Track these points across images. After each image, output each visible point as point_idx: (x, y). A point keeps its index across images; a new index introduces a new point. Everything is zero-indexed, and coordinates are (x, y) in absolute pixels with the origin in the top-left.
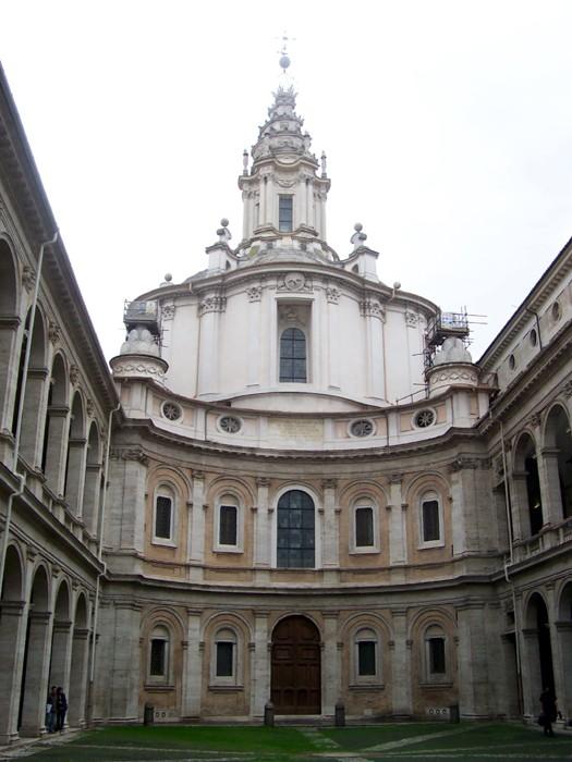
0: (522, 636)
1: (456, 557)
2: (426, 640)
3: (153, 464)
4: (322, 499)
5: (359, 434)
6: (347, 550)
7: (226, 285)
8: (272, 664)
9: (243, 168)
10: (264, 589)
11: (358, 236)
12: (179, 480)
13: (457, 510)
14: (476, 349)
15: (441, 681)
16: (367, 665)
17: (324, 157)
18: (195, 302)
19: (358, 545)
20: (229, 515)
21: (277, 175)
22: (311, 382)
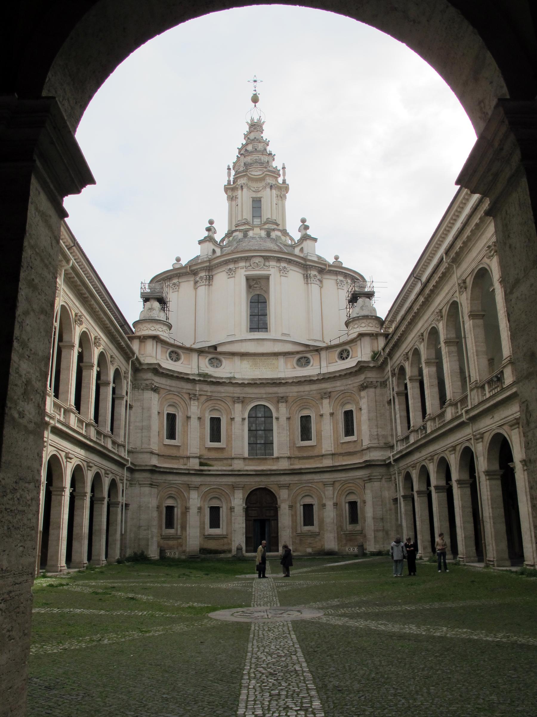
0: (402, 500)
1: (364, 447)
3: (162, 392)
4: (278, 409)
5: (301, 366)
6: (294, 444)
8: (246, 520)
10: (239, 471)
11: (303, 226)
12: (182, 403)
14: (382, 306)
15: (356, 529)
16: (308, 519)
17: (284, 168)
18: (192, 279)
19: (302, 440)
20: (216, 423)
21: (250, 184)
22: (270, 331)
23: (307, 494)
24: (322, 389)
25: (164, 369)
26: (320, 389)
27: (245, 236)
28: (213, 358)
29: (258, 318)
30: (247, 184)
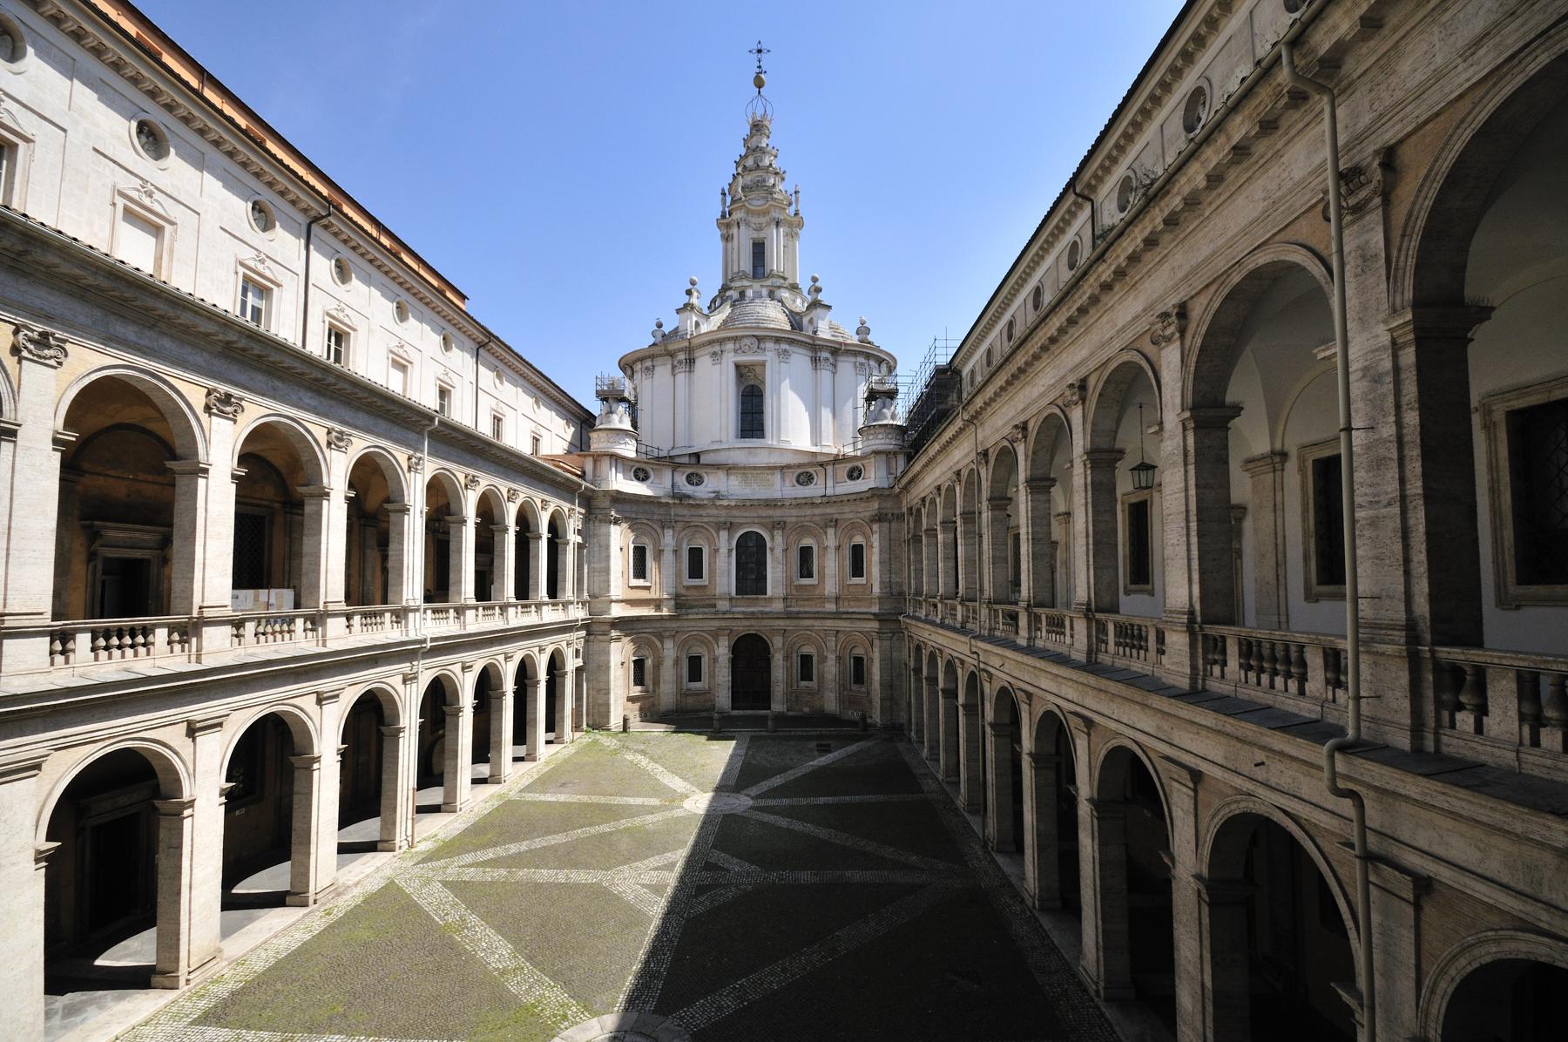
4: (773, 538)
13: (876, 558)
18: (668, 360)
29: (752, 419)
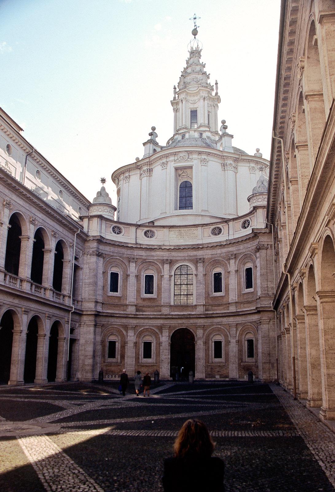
2: (245, 341)
5: (216, 234)
6: (209, 295)
7: (151, 161)
9: (174, 96)
10: (166, 315)
11: (223, 126)
17: (216, 84)
18: (138, 172)
19: (215, 292)
20: (149, 279)
21: (189, 98)
23: (217, 333)
24: (230, 252)
25: (108, 239)
26: (228, 252)
27: (183, 137)
28: (148, 231)
30: (186, 98)
